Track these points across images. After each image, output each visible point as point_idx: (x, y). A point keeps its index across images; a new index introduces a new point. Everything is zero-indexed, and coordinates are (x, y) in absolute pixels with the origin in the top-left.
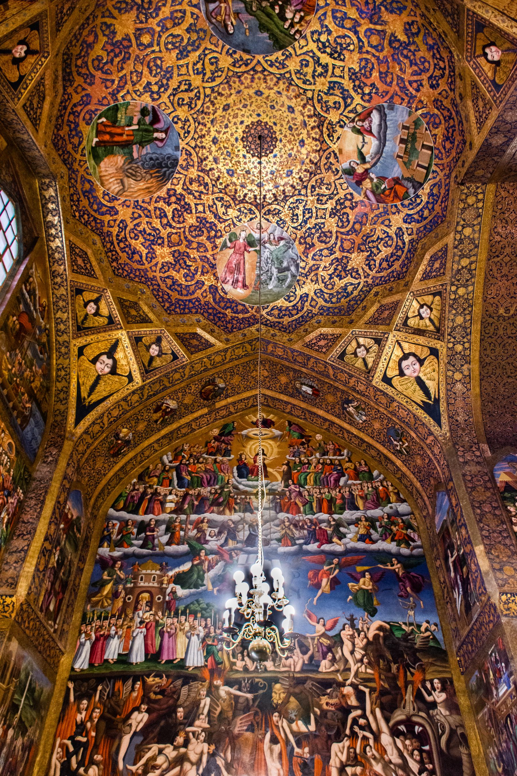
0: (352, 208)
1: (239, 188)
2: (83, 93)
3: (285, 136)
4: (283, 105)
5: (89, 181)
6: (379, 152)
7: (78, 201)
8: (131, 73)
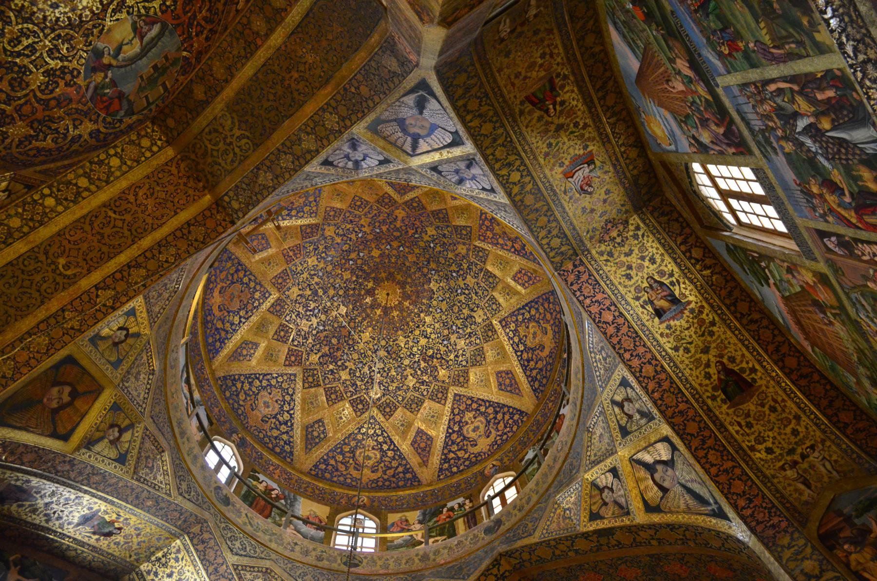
0: (67, 85)
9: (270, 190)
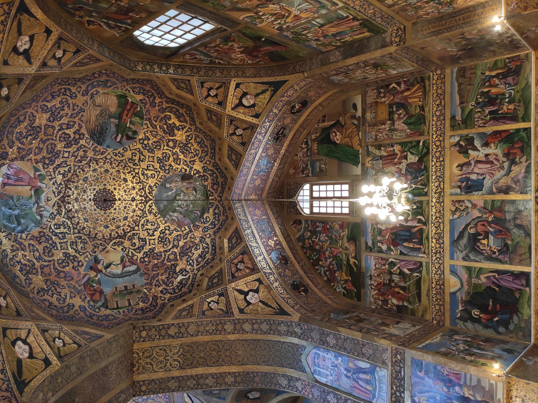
1: (75, 184)
2: (157, 105)
3: (108, 216)
4: (127, 213)
5: (110, 86)
6: (115, 276)
7: (108, 76)
8: (157, 132)
9: (170, 390)
